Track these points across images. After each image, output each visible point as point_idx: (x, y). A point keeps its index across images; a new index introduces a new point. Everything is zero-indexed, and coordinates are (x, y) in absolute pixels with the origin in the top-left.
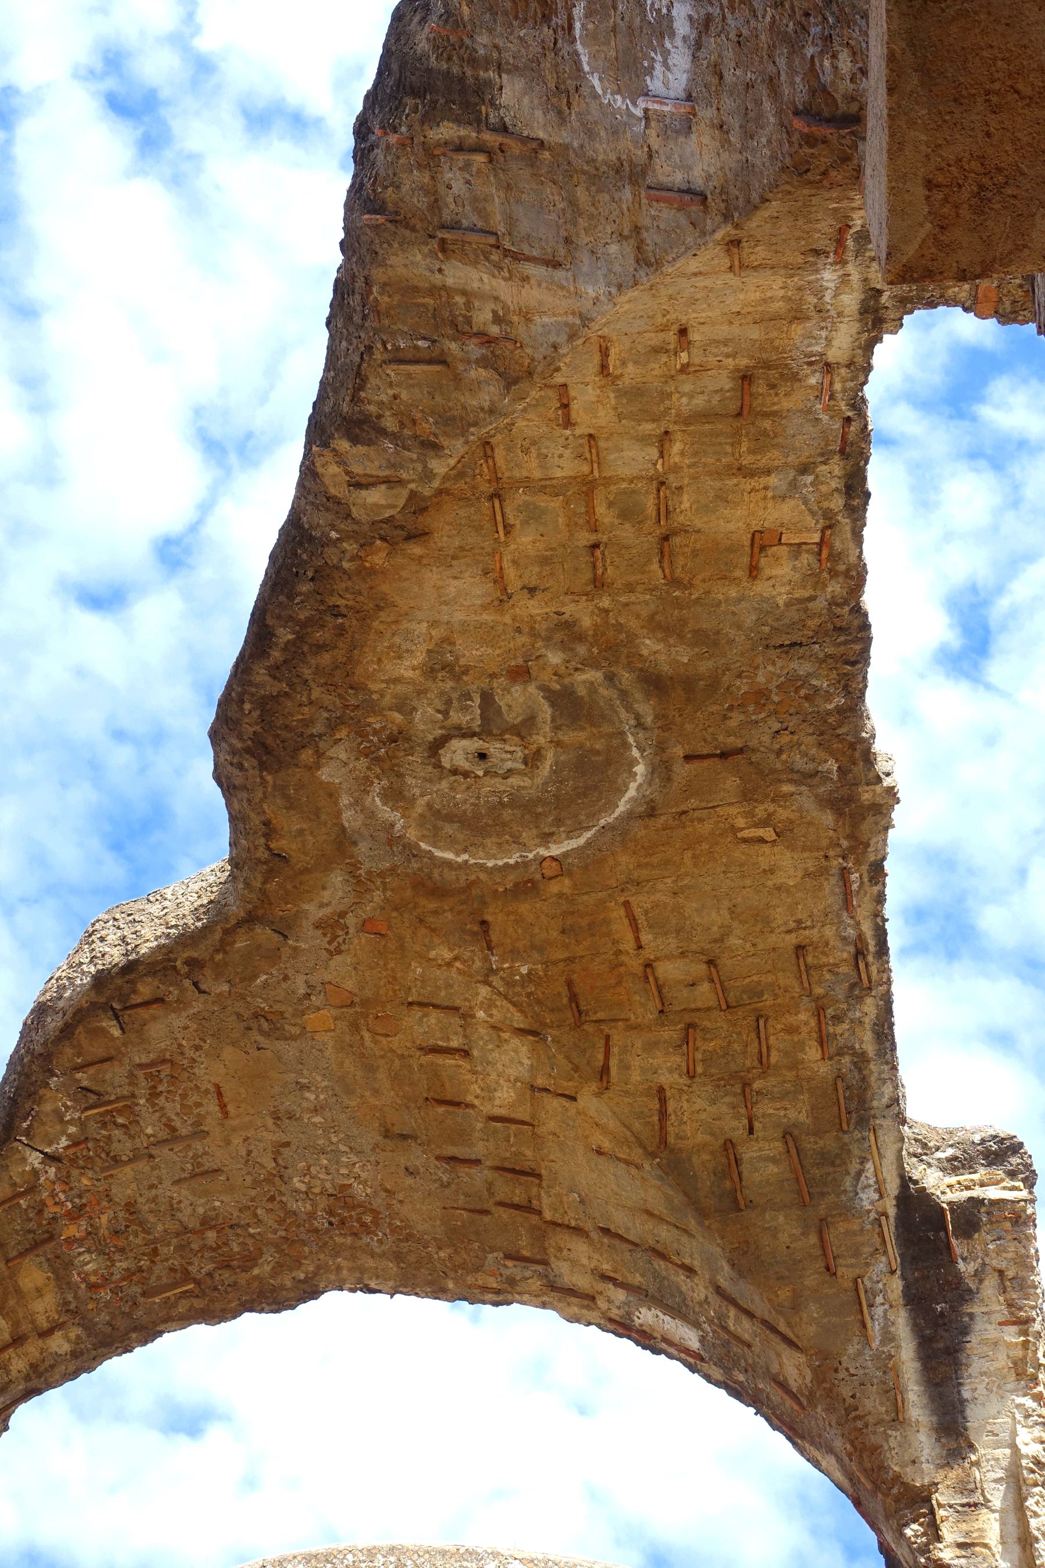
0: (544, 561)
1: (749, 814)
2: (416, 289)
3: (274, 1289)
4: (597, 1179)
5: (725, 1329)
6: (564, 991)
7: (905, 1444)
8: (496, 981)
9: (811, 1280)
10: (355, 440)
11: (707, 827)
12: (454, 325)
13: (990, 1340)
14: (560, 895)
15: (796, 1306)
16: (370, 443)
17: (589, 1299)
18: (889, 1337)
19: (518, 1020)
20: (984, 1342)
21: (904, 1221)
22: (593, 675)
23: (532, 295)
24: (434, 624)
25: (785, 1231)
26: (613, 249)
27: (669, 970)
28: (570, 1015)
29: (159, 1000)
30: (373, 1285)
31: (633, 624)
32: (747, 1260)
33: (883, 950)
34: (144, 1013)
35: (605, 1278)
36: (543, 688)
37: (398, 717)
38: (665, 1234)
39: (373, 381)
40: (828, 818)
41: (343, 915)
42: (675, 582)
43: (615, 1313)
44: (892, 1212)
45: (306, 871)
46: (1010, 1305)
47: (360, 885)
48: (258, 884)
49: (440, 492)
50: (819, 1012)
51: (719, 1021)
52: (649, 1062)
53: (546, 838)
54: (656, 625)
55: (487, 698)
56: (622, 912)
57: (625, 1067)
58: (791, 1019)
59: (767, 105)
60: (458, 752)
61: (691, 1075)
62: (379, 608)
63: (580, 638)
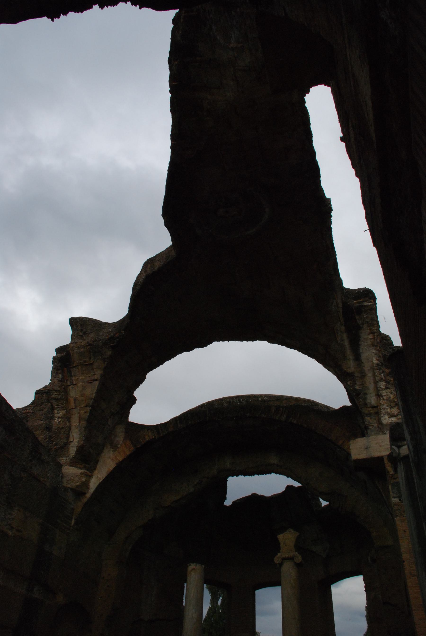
20: (364, 339)
44: (341, 310)
46: (370, 329)
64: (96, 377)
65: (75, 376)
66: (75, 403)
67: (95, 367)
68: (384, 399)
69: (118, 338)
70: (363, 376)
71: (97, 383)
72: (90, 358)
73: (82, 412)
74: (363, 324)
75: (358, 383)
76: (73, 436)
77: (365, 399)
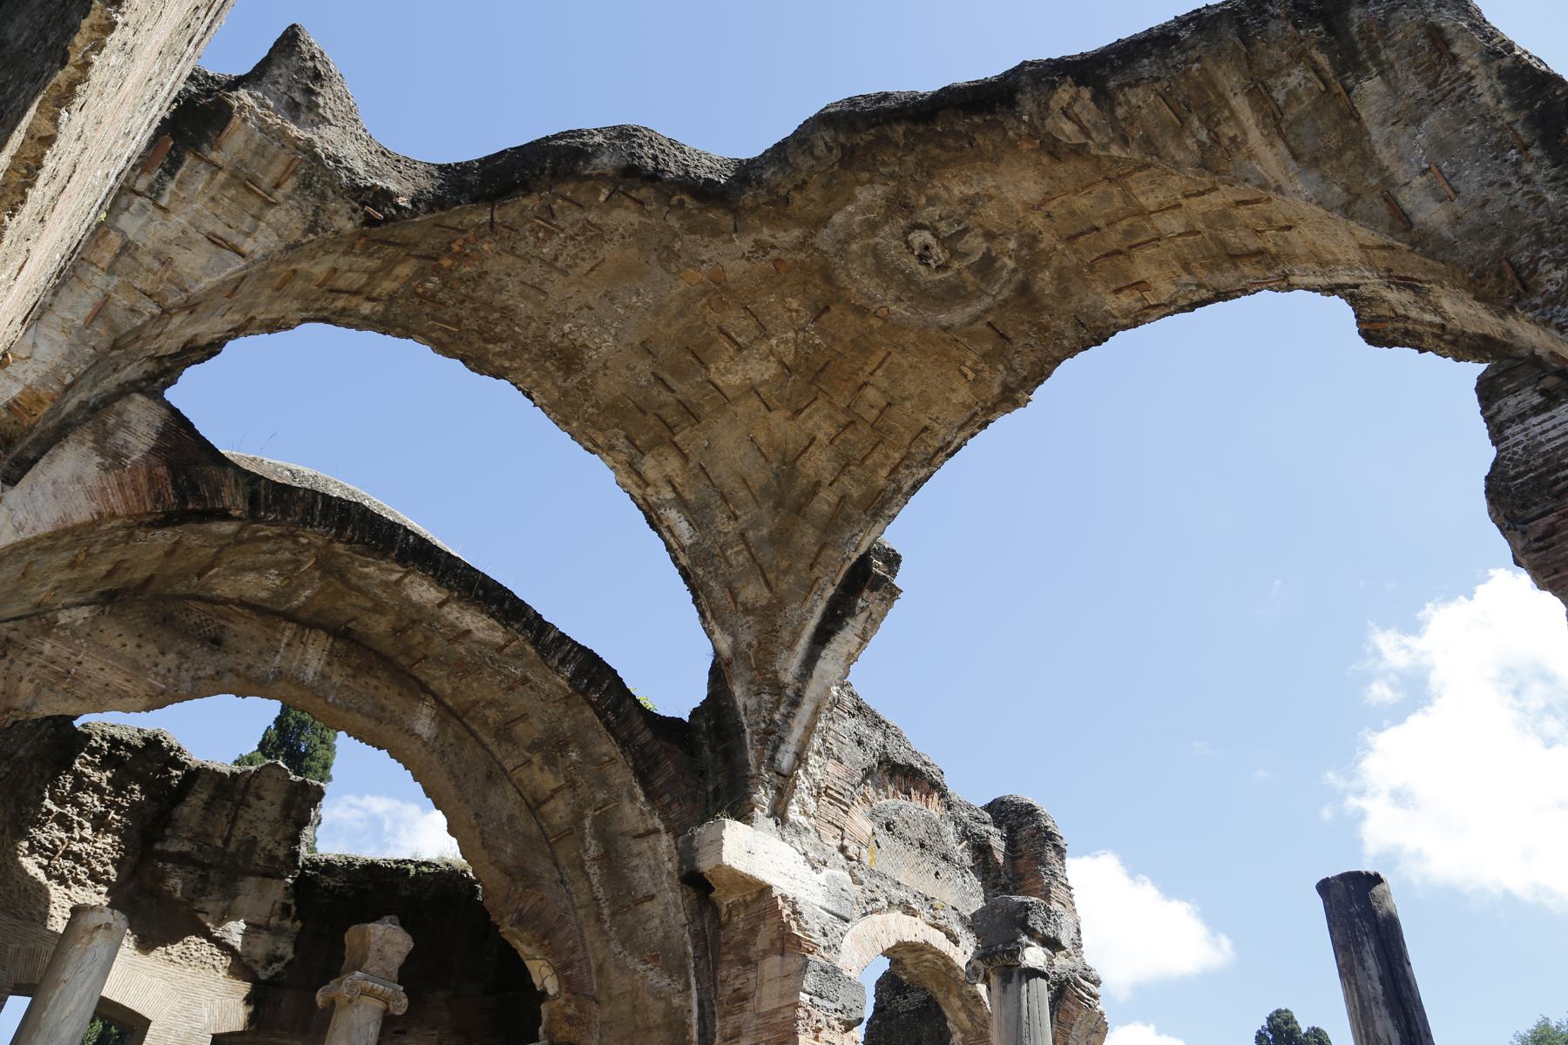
0: (1073, 213)
1: (976, 363)
2: (1215, 87)
3: (487, 361)
4: (732, 448)
5: (723, 552)
6: (822, 364)
8: (801, 335)
9: (800, 566)
10: (1094, 99)
11: (955, 353)
12: (1209, 117)
13: (846, 638)
14: (871, 326)
15: (786, 572)
16: (1099, 106)
18: (811, 611)
21: (854, 567)
22: (1011, 264)
23: (1265, 153)
24: (998, 187)
25: (808, 537)
26: (1337, 189)
27: (871, 394)
28: (810, 377)
29: (641, 203)
30: (534, 395)
31: (1055, 263)
32: (780, 539)
33: (951, 455)
34: (627, 202)
35: (670, 482)
36: (989, 250)
37: (924, 200)
38: (742, 494)
39: (1139, 91)
40: (996, 390)
41: (773, 247)
42: (1091, 267)
43: (653, 499)
45: (789, 217)
47: (802, 245)
48: (761, 201)
49: (1098, 157)
51: (864, 430)
52: (820, 423)
53: (898, 300)
54: (1060, 275)
55: (966, 231)
56: (883, 354)
57: (810, 417)
58: (891, 453)
59: (1496, 241)
60: (920, 238)
61: (831, 442)
62: (991, 160)
63: (1031, 247)
64: (247, 246)
65: (181, 183)
66: (117, 256)
67: (271, 215)
69: (397, 207)
70: (795, 703)
71: (238, 264)
72: (277, 186)
73: (121, 300)
74: (863, 609)
75: (782, 709)
76: (35, 345)
77: (776, 749)
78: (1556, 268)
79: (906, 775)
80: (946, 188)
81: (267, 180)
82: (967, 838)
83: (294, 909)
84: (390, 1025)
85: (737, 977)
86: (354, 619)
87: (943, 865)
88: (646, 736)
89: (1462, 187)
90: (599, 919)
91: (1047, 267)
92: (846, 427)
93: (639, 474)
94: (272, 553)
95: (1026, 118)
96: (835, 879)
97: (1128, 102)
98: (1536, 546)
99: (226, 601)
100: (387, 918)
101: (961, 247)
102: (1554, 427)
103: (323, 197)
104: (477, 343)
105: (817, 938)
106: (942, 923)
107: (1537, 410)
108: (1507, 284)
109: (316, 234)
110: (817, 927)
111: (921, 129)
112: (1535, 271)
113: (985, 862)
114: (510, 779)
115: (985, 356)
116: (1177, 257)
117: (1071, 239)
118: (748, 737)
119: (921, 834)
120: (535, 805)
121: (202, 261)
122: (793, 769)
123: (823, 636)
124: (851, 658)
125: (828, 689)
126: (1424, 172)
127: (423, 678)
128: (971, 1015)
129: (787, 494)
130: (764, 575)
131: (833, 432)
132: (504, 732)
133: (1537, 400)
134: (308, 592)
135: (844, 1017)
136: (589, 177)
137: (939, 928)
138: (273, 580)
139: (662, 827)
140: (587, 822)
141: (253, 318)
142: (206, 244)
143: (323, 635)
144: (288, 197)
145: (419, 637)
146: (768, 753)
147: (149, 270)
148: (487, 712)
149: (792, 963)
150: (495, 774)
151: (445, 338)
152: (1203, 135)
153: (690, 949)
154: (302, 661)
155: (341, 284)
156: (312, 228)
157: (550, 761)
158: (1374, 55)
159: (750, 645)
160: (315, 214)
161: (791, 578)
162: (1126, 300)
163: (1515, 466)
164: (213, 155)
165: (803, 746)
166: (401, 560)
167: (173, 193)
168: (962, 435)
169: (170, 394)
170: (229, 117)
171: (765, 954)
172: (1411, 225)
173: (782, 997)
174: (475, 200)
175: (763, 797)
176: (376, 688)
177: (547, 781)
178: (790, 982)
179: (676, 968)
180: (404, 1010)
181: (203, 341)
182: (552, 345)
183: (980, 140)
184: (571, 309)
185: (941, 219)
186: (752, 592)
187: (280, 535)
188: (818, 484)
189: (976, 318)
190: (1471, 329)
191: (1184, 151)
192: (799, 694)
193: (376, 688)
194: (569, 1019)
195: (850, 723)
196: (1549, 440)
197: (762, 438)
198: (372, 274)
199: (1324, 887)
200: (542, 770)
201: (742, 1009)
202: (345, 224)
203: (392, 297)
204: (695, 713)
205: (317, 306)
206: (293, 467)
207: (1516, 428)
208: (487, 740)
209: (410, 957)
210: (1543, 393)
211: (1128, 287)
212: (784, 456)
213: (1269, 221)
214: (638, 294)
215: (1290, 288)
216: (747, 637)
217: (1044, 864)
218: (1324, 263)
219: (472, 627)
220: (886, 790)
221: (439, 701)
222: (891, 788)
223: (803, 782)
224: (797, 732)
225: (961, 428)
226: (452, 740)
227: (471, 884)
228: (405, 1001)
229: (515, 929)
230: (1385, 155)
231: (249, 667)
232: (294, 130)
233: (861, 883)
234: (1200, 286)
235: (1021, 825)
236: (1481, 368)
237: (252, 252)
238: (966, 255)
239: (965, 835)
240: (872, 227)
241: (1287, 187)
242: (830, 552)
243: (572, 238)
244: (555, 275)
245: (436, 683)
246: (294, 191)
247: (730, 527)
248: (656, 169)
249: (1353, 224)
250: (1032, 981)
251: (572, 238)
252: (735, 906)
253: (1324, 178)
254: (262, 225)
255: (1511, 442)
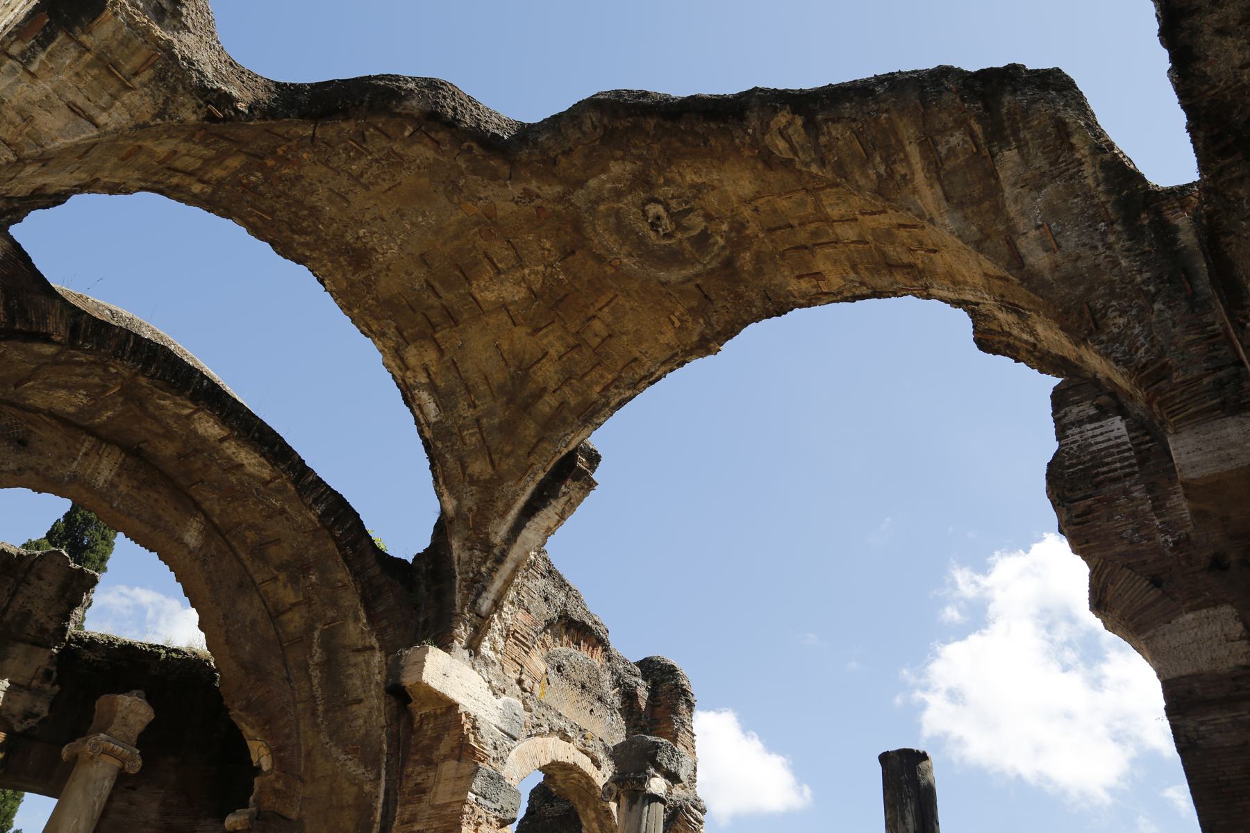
0: (775, 211)
1: (682, 315)
2: (896, 134)
4: (480, 350)
5: (460, 432)
7: (498, 525)
8: (549, 269)
10: (805, 126)
13: (547, 515)
14: (605, 272)
15: (508, 456)
17: (405, 367)
18: (523, 489)
19: (536, 287)
22: (721, 242)
23: (926, 192)
24: (720, 181)
25: (529, 430)
26: (974, 228)
27: (597, 325)
28: (551, 304)
29: (438, 143)
31: (755, 247)
32: (508, 429)
34: (427, 140)
35: (426, 369)
36: (706, 228)
37: (662, 181)
38: (483, 388)
39: (840, 126)
40: (695, 338)
41: (538, 197)
47: (561, 199)
48: (534, 158)
49: (800, 171)
50: (614, 380)
52: (553, 341)
53: (630, 255)
54: (758, 257)
55: (691, 210)
57: (546, 335)
58: (606, 374)
59: (1082, 288)
60: (655, 209)
62: (719, 159)
64: (102, 118)
65: (51, 56)
67: (126, 97)
68: (500, 615)
70: (500, 561)
71: (92, 132)
72: (136, 74)
74: (565, 494)
75: (488, 564)
77: (479, 595)
78: (1120, 316)
79: (580, 631)
80: (681, 175)
81: (128, 67)
82: (620, 686)
83: (55, 674)
84: (123, 781)
85: (419, 774)
86: (145, 441)
87: (598, 704)
88: (375, 570)
89: (1063, 244)
90: (314, 713)
91: (749, 249)
92: (573, 348)
93: (402, 359)
94: (84, 376)
95: (750, 131)
96: (510, 705)
97: (829, 133)
98: (1075, 520)
99: (37, 411)
100: (135, 692)
101: (685, 222)
102: (1102, 434)
103: (174, 90)
104: (286, 233)
105: (489, 750)
106: (590, 750)
107: (1092, 419)
108: (1084, 322)
109: (164, 119)
110: (490, 742)
111: (668, 124)
112: (1105, 315)
113: (631, 706)
114: (257, 590)
115: (691, 310)
116: (849, 259)
117: (771, 230)
118: (458, 582)
119: (584, 677)
120: (275, 614)
121: (60, 124)
122: (490, 612)
123: (530, 511)
124: (550, 531)
125: (527, 553)
126: (1038, 227)
127: (198, 498)
128: (602, 826)
129: (519, 393)
130: (490, 455)
131: (562, 350)
132: (258, 552)
133: (1093, 412)
134: (109, 413)
135: (501, 816)
136: (399, 115)
137: (586, 753)
138: (81, 398)
139: (377, 646)
140: (316, 634)
141: (98, 179)
142: (66, 111)
143: (117, 450)
144: (144, 85)
145: (199, 464)
146: (471, 597)
147: (11, 123)
148: (247, 533)
149: (466, 768)
150: (246, 585)
151: (259, 224)
152: (882, 169)
153: (385, 747)
154: (95, 469)
155: (178, 164)
156: (160, 114)
157: (293, 581)
158: (1015, 132)
159: (470, 509)
160: (165, 103)
161: (512, 461)
162: (805, 285)
163: (1070, 459)
164: (83, 38)
165: (501, 595)
166: (194, 399)
167: (42, 62)
168: (663, 369)
169: (15, 231)
170: (103, 9)
171: (446, 758)
172: (1023, 265)
173: (453, 794)
174: (302, 116)
175: (463, 631)
176: (156, 500)
177: (288, 596)
178: (462, 783)
179: (371, 761)
180: (137, 770)
181: (51, 191)
182: (347, 244)
183: (713, 142)
184: (368, 217)
185: (673, 197)
186: (479, 467)
187: (92, 362)
188: (544, 390)
189: (688, 280)
190: (1054, 351)
191: (867, 178)
192: (504, 554)
193: (156, 500)
194: (276, 792)
195: (541, 582)
196: (1097, 443)
197: (505, 347)
198: (206, 161)
199: (885, 758)
200: (285, 586)
201: (420, 800)
202: (189, 115)
203: (220, 183)
204: (418, 557)
205: (155, 179)
206: (113, 308)
207: (1075, 430)
208: (243, 555)
209: (150, 727)
210: (1098, 407)
211: (808, 275)
212: (521, 363)
213: (921, 243)
214: (424, 215)
215: (929, 297)
216: (469, 502)
217: (676, 714)
218: (956, 283)
219: (245, 462)
220: (561, 639)
221: (207, 517)
222: (565, 638)
223: (497, 625)
224: (498, 584)
225: (663, 363)
226: (214, 552)
227: (212, 671)
228: (139, 763)
229: (243, 714)
230: (1012, 210)
231: (48, 468)
232: (158, 31)
233: (531, 711)
234: (862, 283)
235: (663, 681)
236: (1057, 381)
237: (106, 124)
238: (687, 229)
239: (619, 683)
240: (618, 194)
241: (938, 220)
242: (545, 445)
243: (377, 161)
244: (359, 189)
245: (208, 503)
246: (150, 81)
247: (468, 413)
248: (454, 118)
249: (981, 257)
250: (653, 805)
251: (377, 161)
252: (427, 716)
253: (966, 218)
254: (118, 104)
255: (1070, 440)
